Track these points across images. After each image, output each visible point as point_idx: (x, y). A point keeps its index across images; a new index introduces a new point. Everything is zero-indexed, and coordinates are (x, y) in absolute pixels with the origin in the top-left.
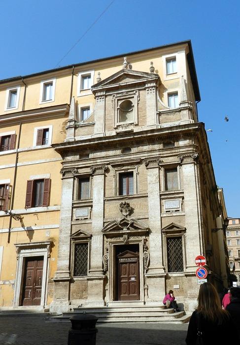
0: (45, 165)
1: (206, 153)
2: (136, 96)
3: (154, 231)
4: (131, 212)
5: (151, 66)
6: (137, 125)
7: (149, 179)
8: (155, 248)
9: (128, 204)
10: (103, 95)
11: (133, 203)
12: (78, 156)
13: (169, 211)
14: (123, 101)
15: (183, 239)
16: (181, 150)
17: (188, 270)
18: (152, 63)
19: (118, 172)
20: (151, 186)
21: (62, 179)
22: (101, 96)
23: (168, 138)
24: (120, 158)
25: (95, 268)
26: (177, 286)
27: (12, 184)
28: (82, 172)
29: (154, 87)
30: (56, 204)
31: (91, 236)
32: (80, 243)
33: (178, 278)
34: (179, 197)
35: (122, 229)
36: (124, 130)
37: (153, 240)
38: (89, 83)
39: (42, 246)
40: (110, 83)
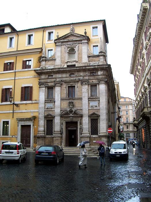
0: (28, 79)
1: (111, 76)
2: (77, 47)
4: (73, 106)
5: (85, 31)
6: (77, 62)
7: (83, 91)
8: (86, 123)
9: (73, 103)
10: (60, 45)
11: (75, 101)
12: (47, 76)
13: (92, 107)
14: (70, 48)
15: (98, 120)
16: (99, 77)
17: (100, 134)
18: (85, 30)
19: (67, 86)
20: (84, 93)
21: (39, 88)
22: (59, 45)
23: (93, 71)
24: (68, 79)
25: (56, 132)
27: (13, 88)
28: (50, 84)
29: (86, 43)
31: (55, 116)
32: (49, 120)
34: (97, 100)
36: (71, 64)
37: (85, 120)
38: (54, 37)
40: (64, 39)
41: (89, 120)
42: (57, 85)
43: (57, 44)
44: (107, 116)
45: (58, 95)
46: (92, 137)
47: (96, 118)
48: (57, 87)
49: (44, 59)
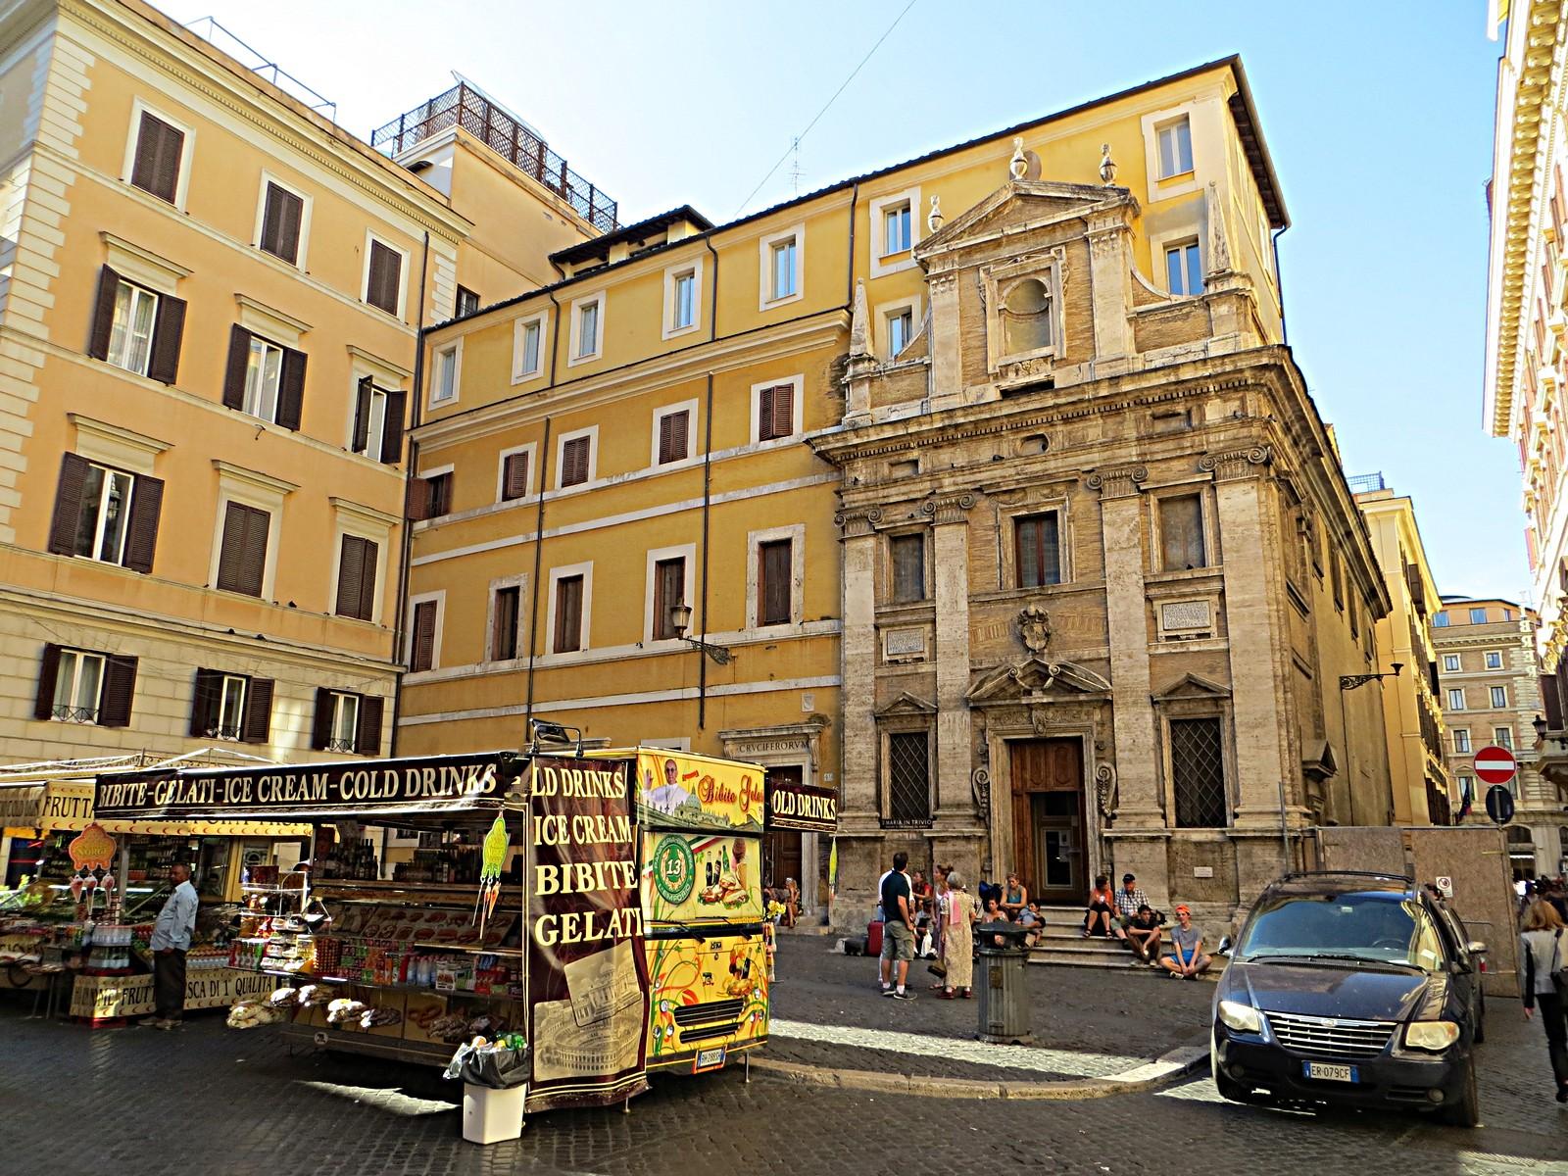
2: (1057, 268)
3: (1130, 700)
10: (951, 273)
11: (1055, 610)
12: (885, 470)
13: (1177, 638)
26: (1208, 871)
28: (899, 517)
30: (826, 614)
31: (937, 710)
33: (1208, 847)
34: (1209, 593)
35: (1029, 693)
36: (1023, 380)
39: (794, 736)
41: (1158, 730)
42: (945, 514)
43: (932, 272)
44: (1280, 695)
45: (953, 579)
46: (1186, 842)
47: (1205, 711)
48: (946, 529)
49: (861, 367)
